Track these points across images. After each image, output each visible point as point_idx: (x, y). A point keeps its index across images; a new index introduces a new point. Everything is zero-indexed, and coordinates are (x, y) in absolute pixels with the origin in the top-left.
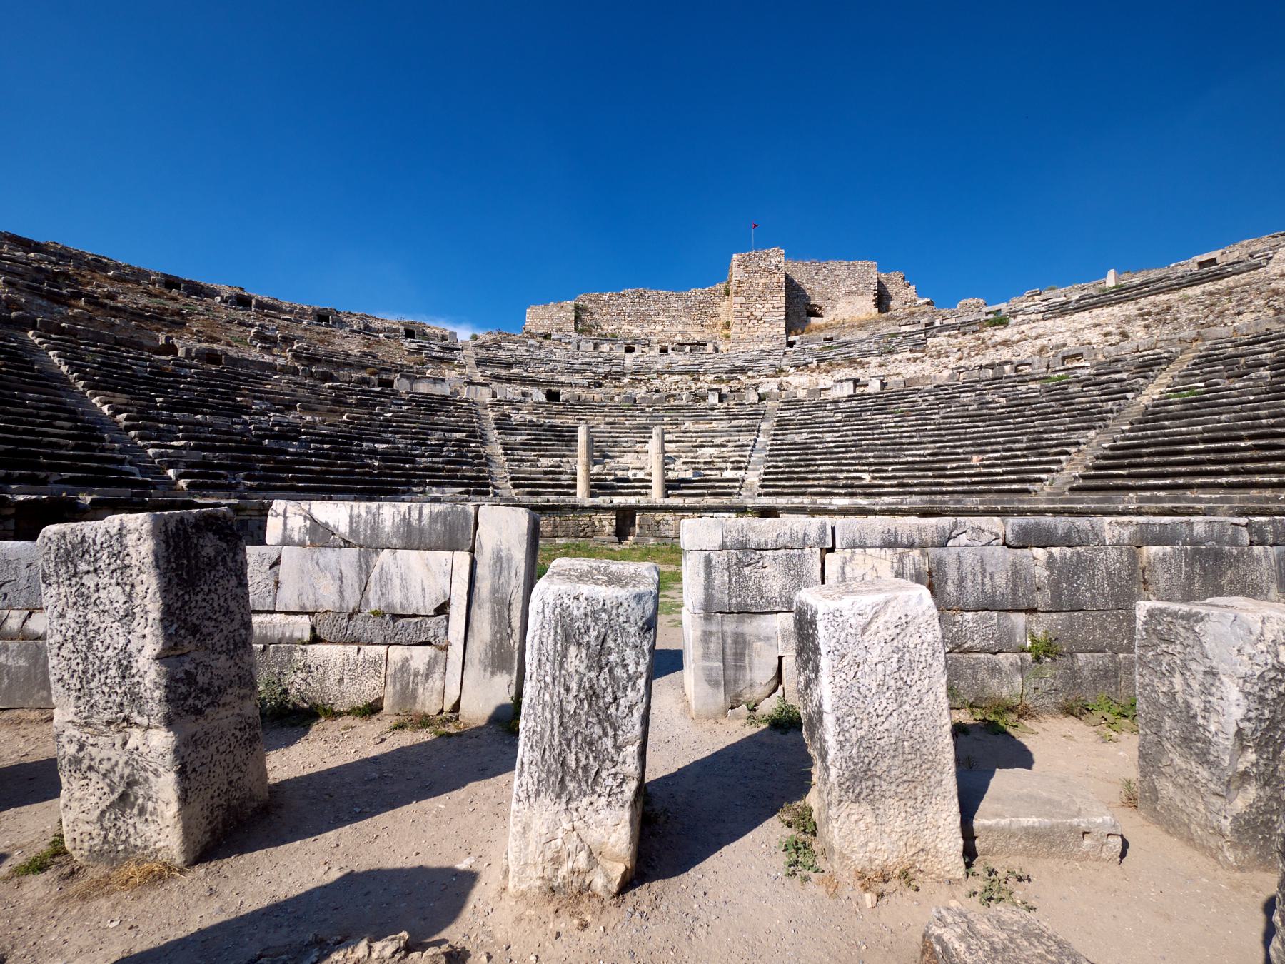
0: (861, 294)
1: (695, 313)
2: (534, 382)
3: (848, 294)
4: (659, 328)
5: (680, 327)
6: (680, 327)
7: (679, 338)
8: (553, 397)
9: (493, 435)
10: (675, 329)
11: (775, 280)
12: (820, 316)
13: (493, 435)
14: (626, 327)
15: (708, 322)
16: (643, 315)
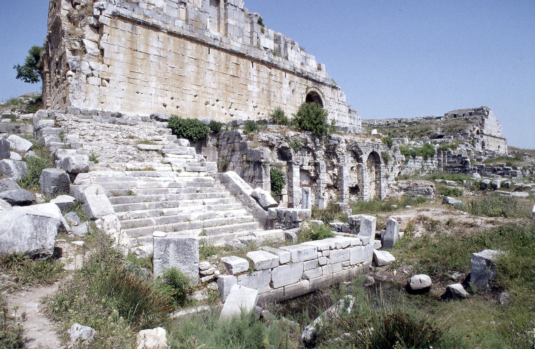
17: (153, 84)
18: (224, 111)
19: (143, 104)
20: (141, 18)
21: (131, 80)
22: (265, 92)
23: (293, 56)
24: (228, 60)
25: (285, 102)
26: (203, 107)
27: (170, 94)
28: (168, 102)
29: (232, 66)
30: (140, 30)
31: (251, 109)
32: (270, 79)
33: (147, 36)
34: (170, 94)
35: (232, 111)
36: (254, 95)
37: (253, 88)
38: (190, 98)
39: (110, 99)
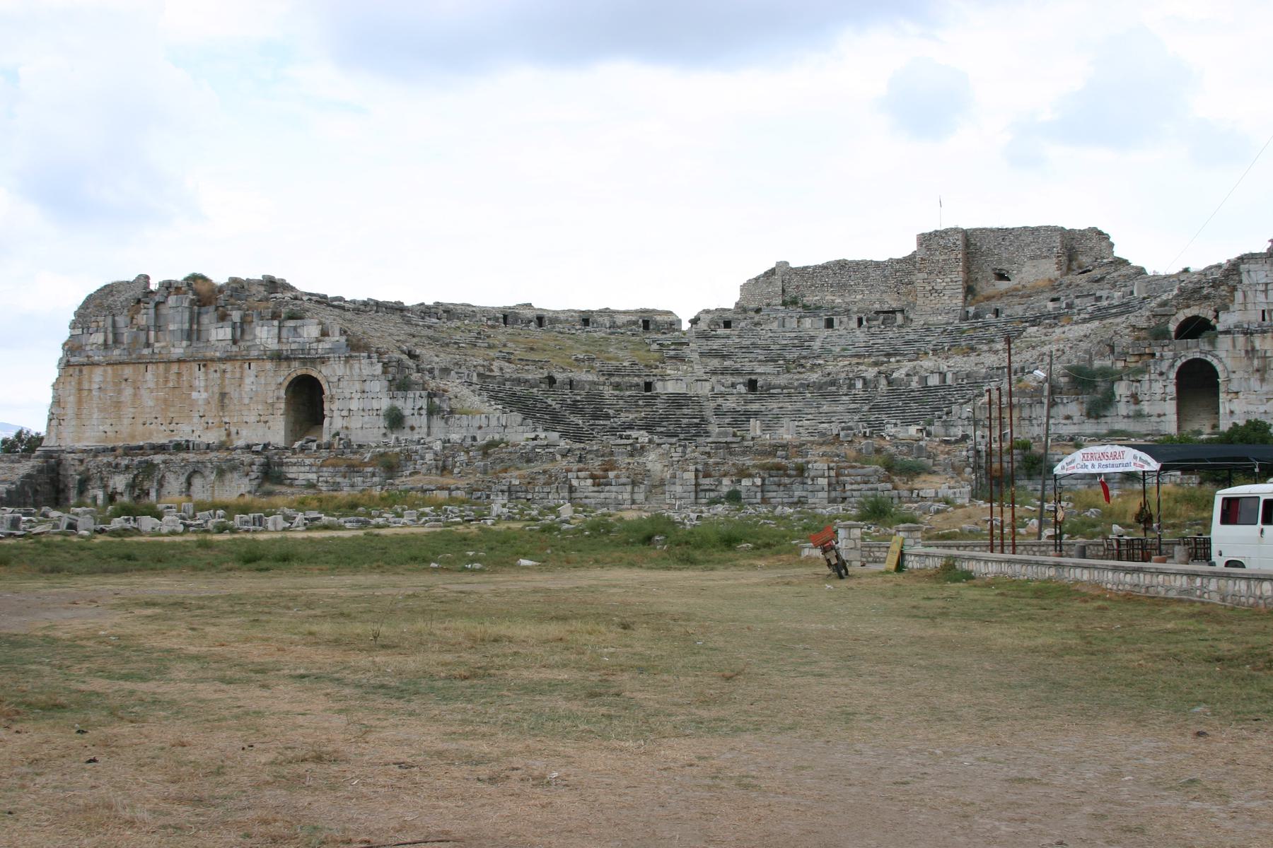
0: (1045, 257)
1: (892, 282)
2: (737, 372)
3: (1032, 258)
4: (859, 297)
5: (878, 295)
6: (878, 295)
7: (877, 306)
8: (752, 385)
9: (713, 419)
10: (873, 297)
11: (953, 256)
12: (1008, 279)
13: (713, 419)
14: (829, 297)
15: (903, 289)
16: (844, 285)
17: (95, 416)
18: (163, 428)
19: (87, 435)
20: (85, 360)
21: (78, 416)
22: (217, 396)
23: (264, 335)
24: (167, 371)
25: (246, 401)
26: (141, 427)
27: (109, 422)
28: (108, 428)
29: (172, 377)
30: (86, 370)
31: (196, 420)
32: (223, 379)
33: (91, 373)
34: (109, 422)
35: (171, 427)
36: (200, 402)
37: (199, 396)
38: (126, 421)
39: (65, 435)
